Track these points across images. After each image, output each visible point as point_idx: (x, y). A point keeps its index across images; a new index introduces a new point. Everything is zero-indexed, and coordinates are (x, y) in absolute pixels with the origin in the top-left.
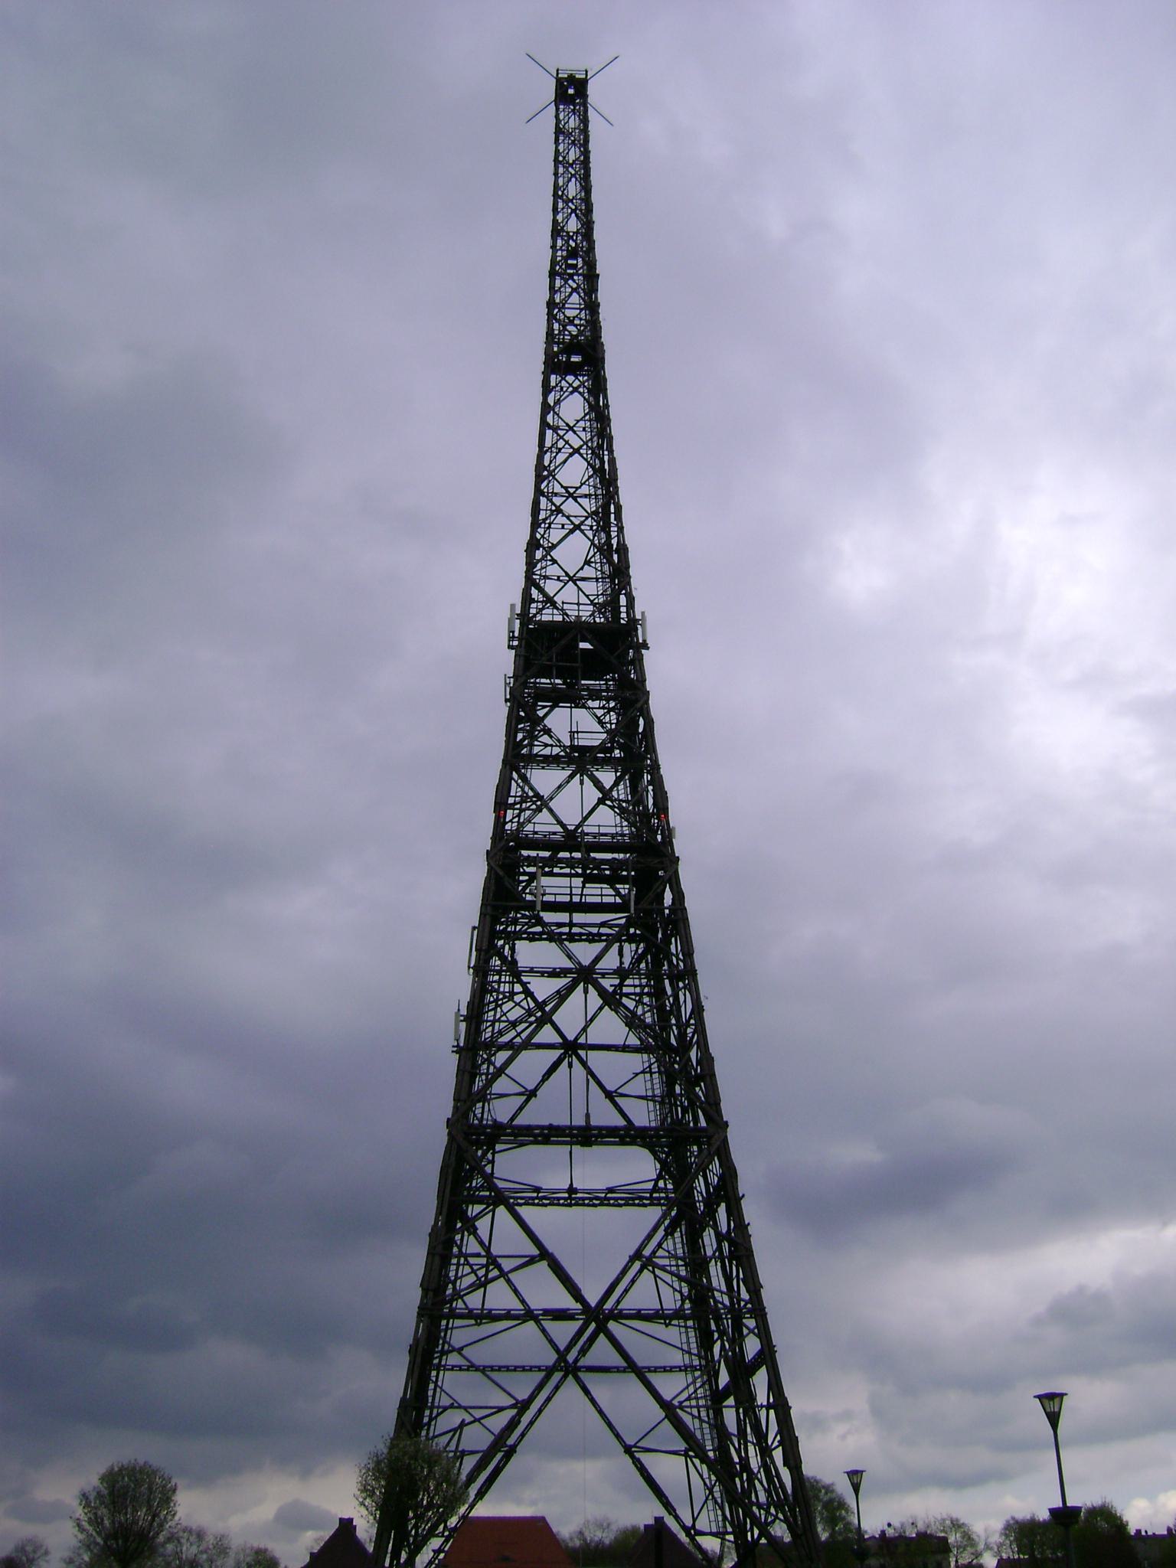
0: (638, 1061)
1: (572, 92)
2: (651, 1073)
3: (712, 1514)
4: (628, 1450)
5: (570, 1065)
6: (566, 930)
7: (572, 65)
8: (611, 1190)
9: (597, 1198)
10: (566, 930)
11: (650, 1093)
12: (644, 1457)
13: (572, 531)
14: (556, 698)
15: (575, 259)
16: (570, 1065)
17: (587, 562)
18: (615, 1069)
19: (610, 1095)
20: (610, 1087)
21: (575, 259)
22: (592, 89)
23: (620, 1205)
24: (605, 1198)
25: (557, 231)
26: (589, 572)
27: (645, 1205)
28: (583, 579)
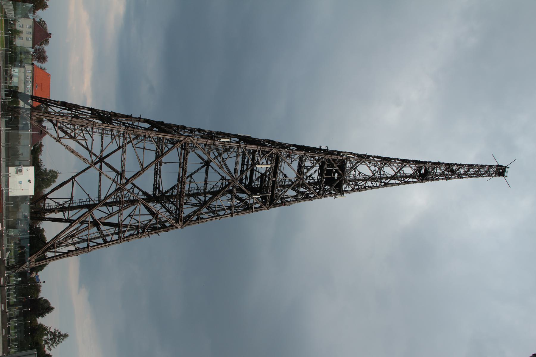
0: (201, 185)
1: (501, 171)
2: (197, 190)
3: (51, 204)
4: (73, 178)
5: (201, 163)
6: (246, 163)
7: (508, 172)
8: (160, 177)
9: (157, 170)
10: (246, 163)
11: (190, 189)
12: (70, 183)
13: (373, 173)
14: (321, 168)
15: (452, 171)
16: (201, 163)
17: (360, 173)
18: (199, 177)
19: (191, 176)
20: (193, 176)
21: (452, 171)
22: (501, 177)
23: (154, 178)
24: (157, 173)
25: (461, 166)
26: (357, 173)
27: (154, 186)
28: (355, 171)
